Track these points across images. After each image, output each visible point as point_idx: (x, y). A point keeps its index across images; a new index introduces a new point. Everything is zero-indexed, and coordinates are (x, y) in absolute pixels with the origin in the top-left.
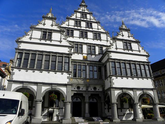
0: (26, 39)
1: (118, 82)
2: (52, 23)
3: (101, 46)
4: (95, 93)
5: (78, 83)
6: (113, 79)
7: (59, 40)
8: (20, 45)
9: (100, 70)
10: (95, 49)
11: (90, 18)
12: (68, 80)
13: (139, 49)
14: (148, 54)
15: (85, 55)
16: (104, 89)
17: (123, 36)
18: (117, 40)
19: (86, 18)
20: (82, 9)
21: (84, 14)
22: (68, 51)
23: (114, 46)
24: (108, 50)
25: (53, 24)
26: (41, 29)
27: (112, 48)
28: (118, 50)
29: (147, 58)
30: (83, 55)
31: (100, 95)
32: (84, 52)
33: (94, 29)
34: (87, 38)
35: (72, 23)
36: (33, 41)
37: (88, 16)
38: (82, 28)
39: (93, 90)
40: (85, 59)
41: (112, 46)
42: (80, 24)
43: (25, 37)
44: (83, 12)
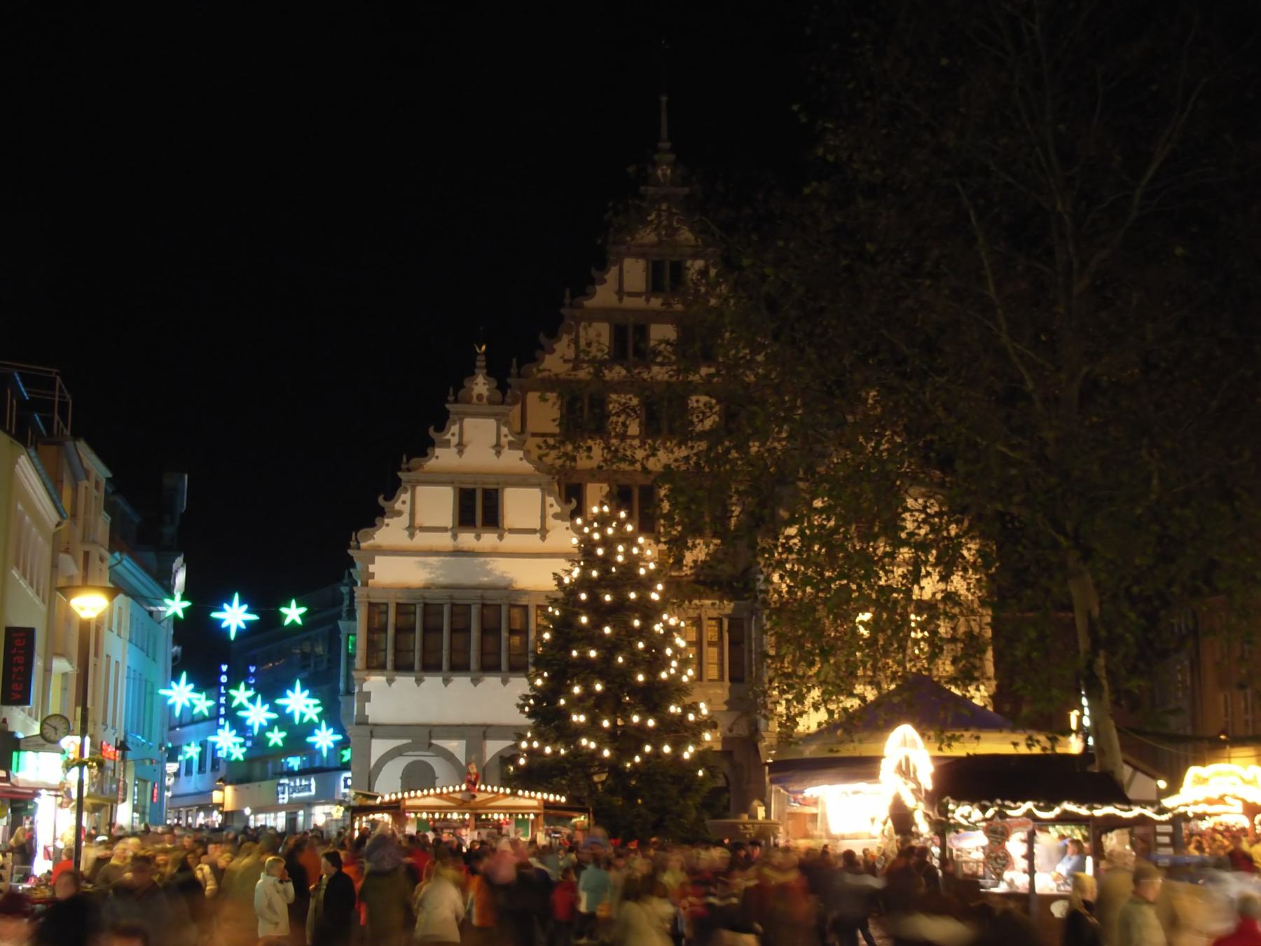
8: (372, 568)
36: (423, 540)
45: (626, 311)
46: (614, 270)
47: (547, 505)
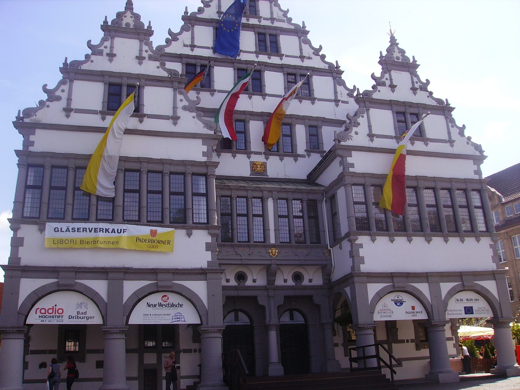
1: (379, 254)
2: (141, 50)
3: (314, 126)
4: (299, 293)
5: (241, 260)
6: (361, 246)
7: (170, 113)
8: (32, 138)
9: (312, 207)
10: (291, 136)
11: (269, 16)
12: (208, 256)
13: (449, 133)
16: (330, 280)
17: (393, 87)
18: (370, 102)
24: (339, 141)
25: (145, 54)
27: (356, 133)
29: (475, 168)
30: (249, 157)
31: (317, 300)
33: (287, 56)
34: (264, 96)
36: (76, 119)
39: (291, 282)
40: (259, 175)
41: (354, 126)
43: (48, 106)
47: (178, 100)
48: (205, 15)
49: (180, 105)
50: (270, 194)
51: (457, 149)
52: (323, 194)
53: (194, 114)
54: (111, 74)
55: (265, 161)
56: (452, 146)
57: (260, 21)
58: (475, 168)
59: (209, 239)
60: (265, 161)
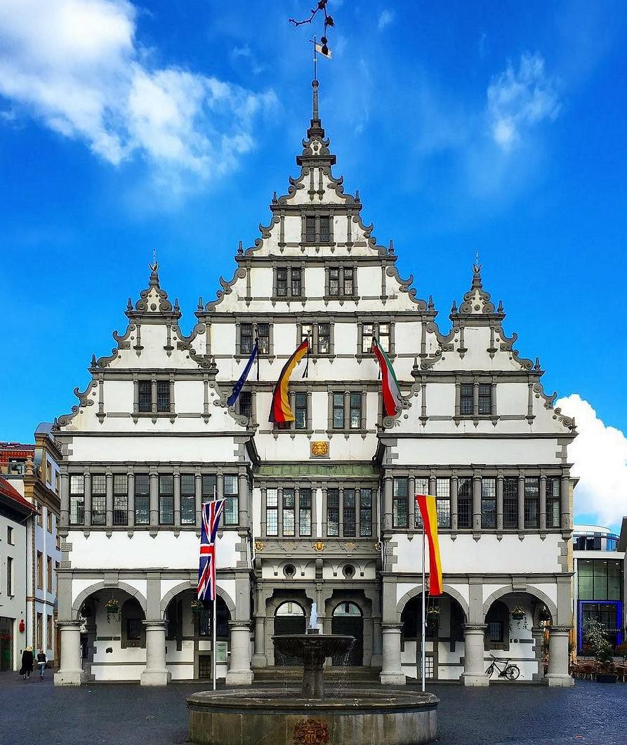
0: (85, 420)
6: (396, 545)
8: (70, 447)
12: (237, 556)
13: (530, 406)
14: (570, 428)
15: (322, 438)
19: (328, 241)
20: (312, 183)
21: (317, 223)
22: (236, 453)
23: (414, 412)
24: (384, 429)
26: (130, 372)
27: (406, 417)
28: (431, 428)
29: (560, 449)
30: (309, 438)
32: (315, 425)
33: (364, 298)
35: (263, 280)
36: (110, 425)
37: (340, 225)
38: (311, 307)
40: (319, 459)
42: (299, 281)
44: (313, 207)
45: (286, 259)
46: (277, 227)
47: (209, 394)
48: (263, 252)
49: (211, 400)
50: (319, 485)
51: (535, 429)
52: (378, 482)
53: (226, 409)
54: (140, 372)
55: (327, 440)
56: (530, 423)
57: (333, 250)
58: (560, 449)
59: (239, 540)
60: (327, 440)
